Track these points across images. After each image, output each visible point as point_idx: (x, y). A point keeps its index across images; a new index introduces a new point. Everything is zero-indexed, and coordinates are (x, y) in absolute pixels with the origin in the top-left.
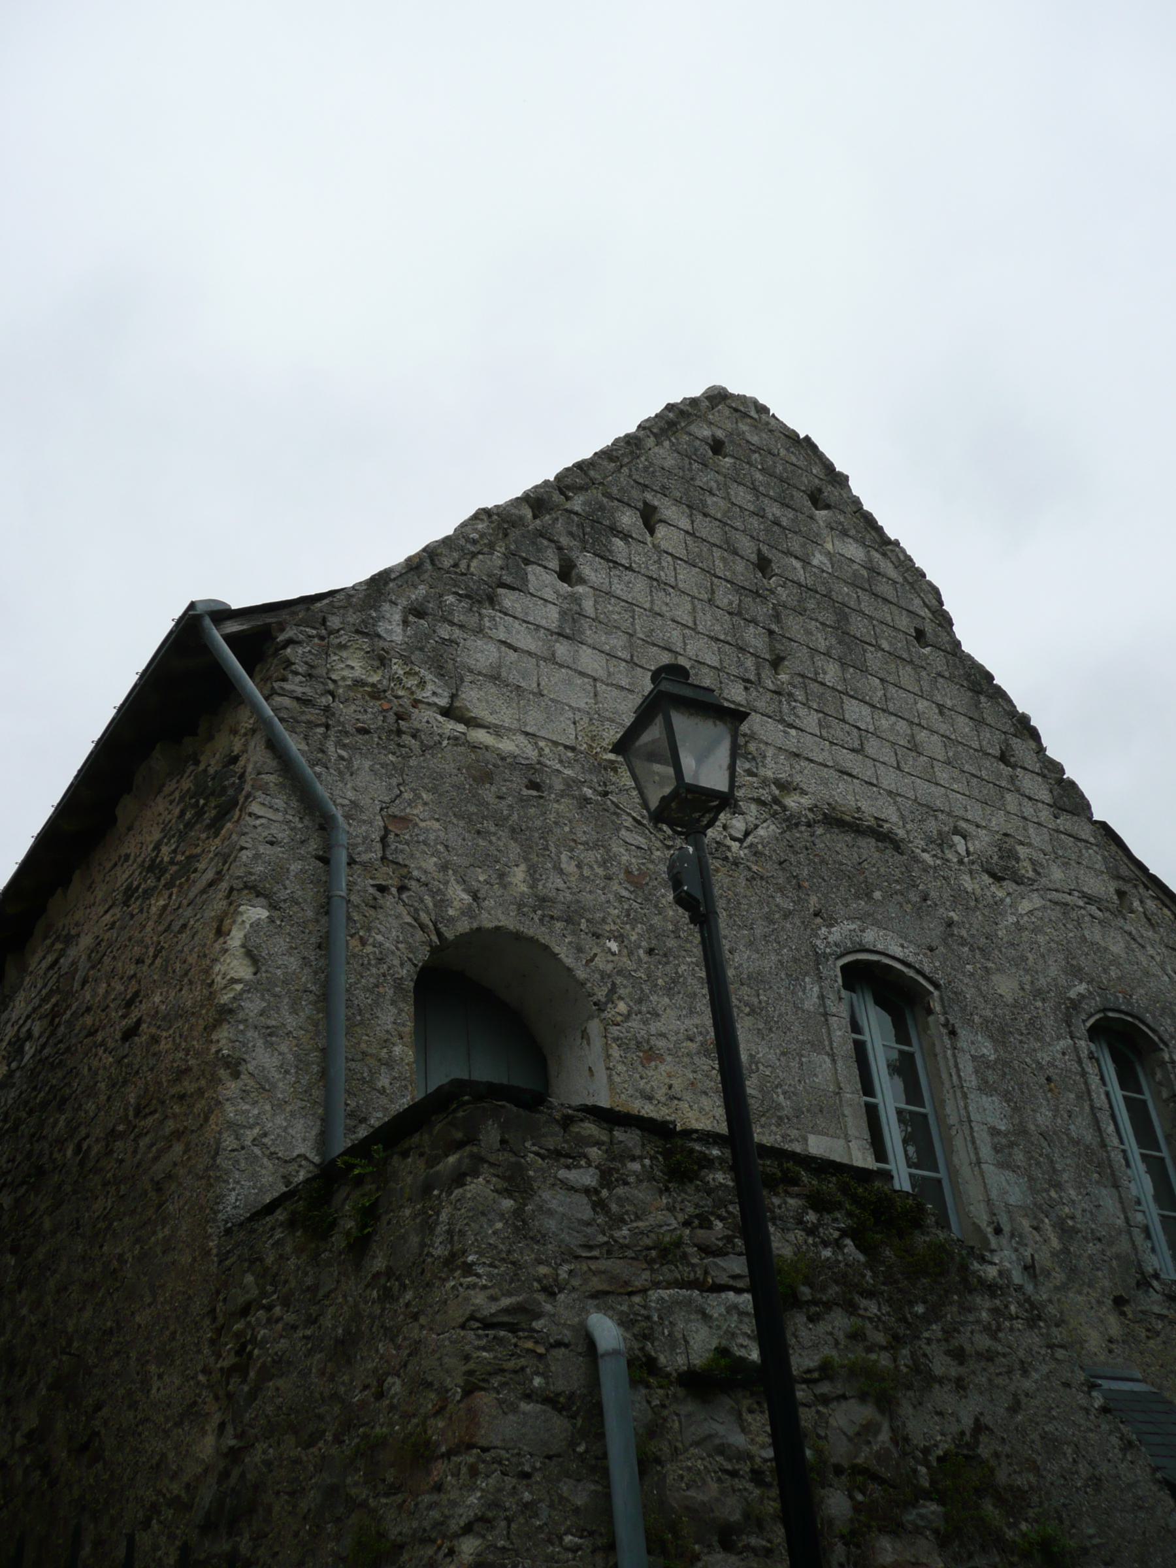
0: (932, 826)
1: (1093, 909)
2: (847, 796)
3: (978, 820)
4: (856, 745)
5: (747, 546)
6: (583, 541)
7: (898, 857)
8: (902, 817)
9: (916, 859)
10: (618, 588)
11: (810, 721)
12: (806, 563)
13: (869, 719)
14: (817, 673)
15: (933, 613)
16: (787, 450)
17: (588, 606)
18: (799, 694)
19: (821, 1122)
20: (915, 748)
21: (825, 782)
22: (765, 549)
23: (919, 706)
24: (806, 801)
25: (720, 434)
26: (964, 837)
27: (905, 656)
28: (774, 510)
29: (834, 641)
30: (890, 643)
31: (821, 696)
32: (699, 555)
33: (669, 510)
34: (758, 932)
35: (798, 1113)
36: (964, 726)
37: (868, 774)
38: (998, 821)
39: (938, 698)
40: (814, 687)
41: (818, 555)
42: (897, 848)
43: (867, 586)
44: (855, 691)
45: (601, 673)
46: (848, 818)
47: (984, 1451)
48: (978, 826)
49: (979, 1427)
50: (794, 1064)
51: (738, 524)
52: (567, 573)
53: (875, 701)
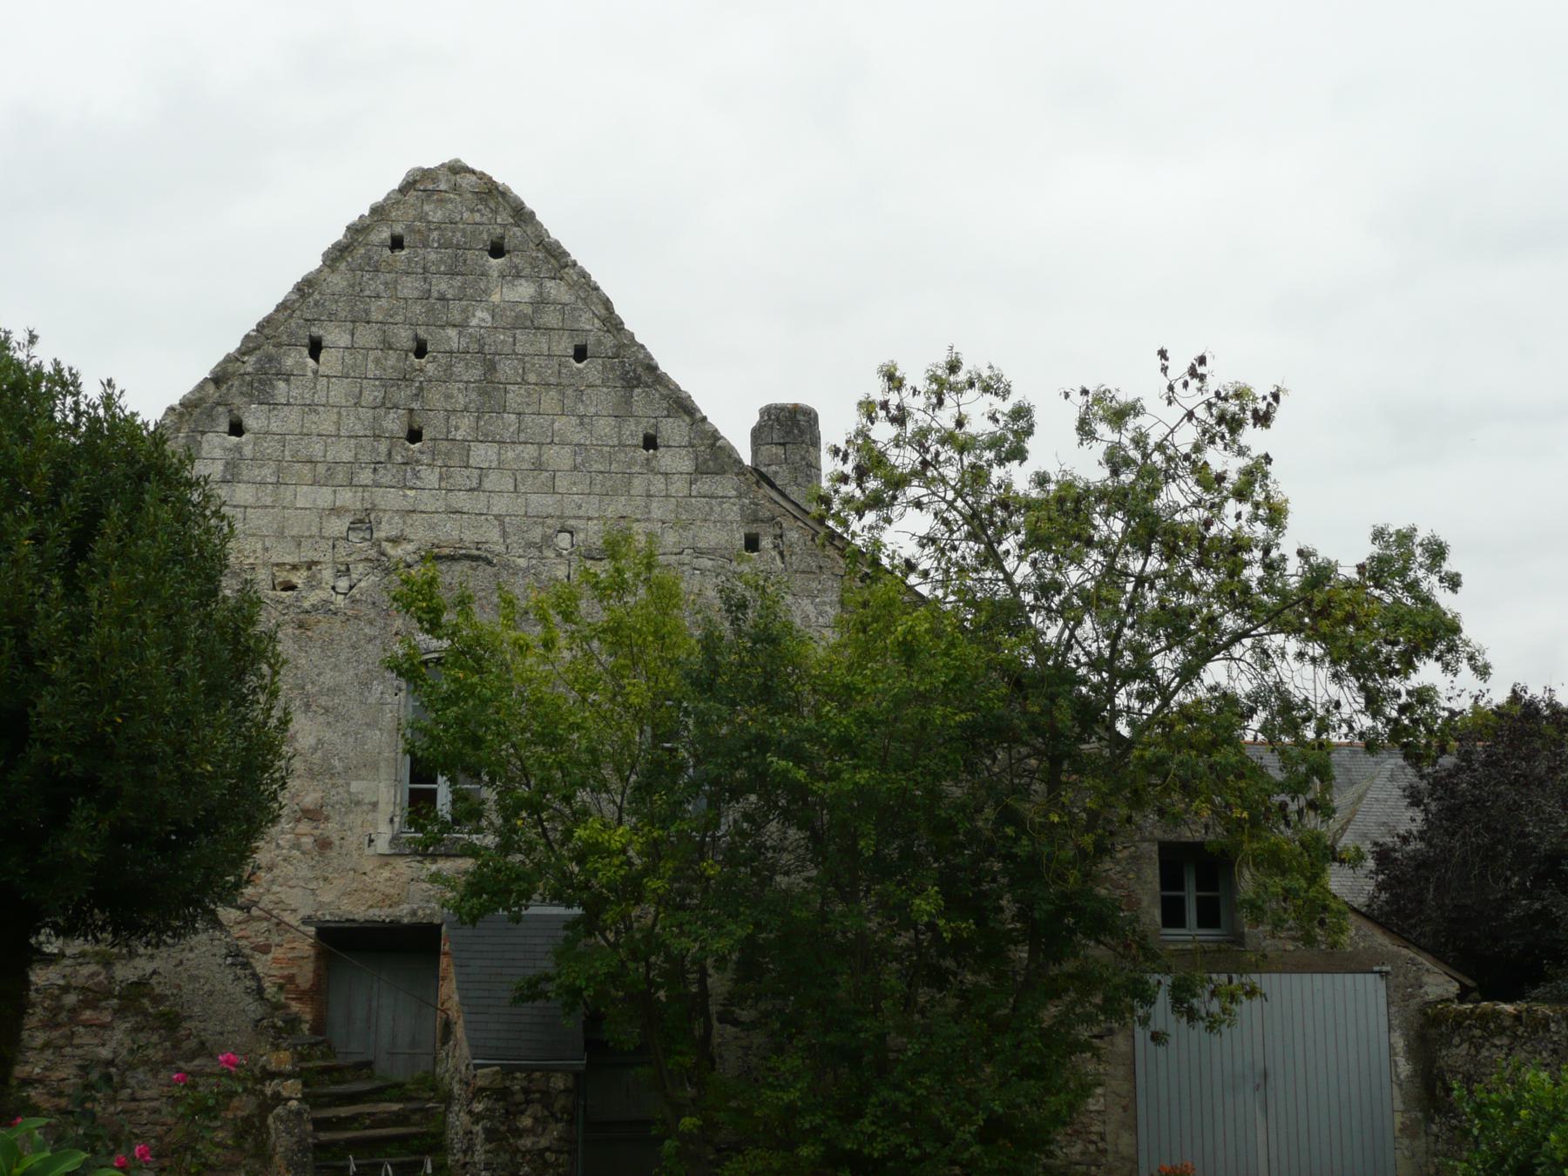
0: (536, 534)
1: (706, 563)
2: (451, 532)
3: (591, 513)
4: (474, 485)
5: (404, 337)
6: (251, 395)
7: (489, 569)
8: (504, 534)
9: (506, 566)
10: (274, 427)
11: (430, 477)
12: (462, 326)
13: (495, 457)
14: (449, 432)
15: (603, 322)
16: (472, 211)
17: (248, 451)
18: (425, 459)
19: (363, 772)
20: (538, 466)
21: (432, 527)
22: (422, 333)
23: (556, 425)
24: (410, 547)
25: (399, 229)
26: (571, 533)
27: (553, 380)
28: (442, 285)
29: (473, 396)
30: (539, 375)
31: (448, 454)
32: (354, 366)
33: (335, 336)
34: (343, 657)
35: (347, 769)
36: (604, 426)
37: (481, 506)
38: (618, 506)
39: (581, 409)
40: (444, 446)
41: (479, 314)
42: (490, 563)
43: (528, 323)
44: (486, 435)
45: (251, 501)
46: (446, 551)
47: (153, 981)
48: (589, 519)
49: (154, 972)
50: (351, 740)
51: (399, 318)
52: (237, 429)
53: (507, 436)
